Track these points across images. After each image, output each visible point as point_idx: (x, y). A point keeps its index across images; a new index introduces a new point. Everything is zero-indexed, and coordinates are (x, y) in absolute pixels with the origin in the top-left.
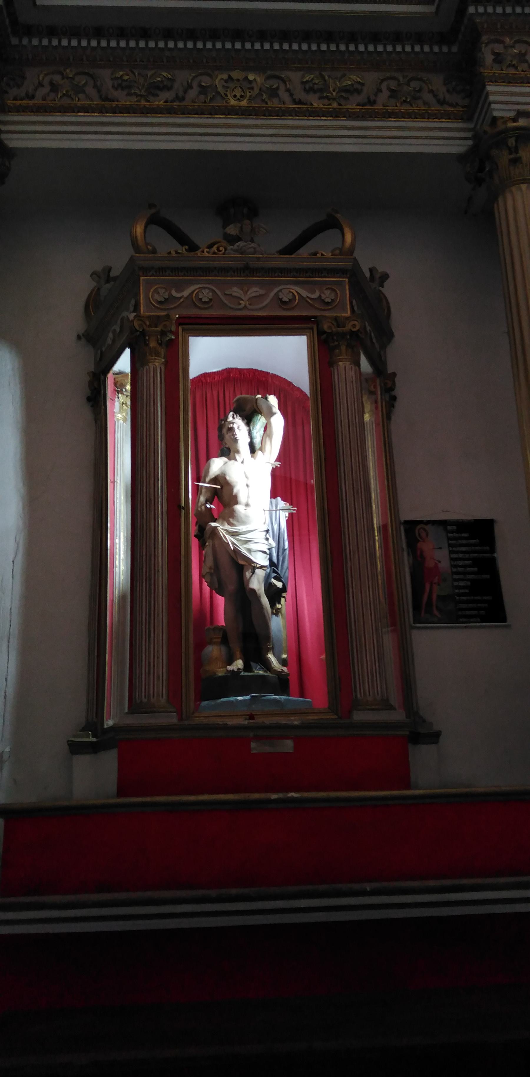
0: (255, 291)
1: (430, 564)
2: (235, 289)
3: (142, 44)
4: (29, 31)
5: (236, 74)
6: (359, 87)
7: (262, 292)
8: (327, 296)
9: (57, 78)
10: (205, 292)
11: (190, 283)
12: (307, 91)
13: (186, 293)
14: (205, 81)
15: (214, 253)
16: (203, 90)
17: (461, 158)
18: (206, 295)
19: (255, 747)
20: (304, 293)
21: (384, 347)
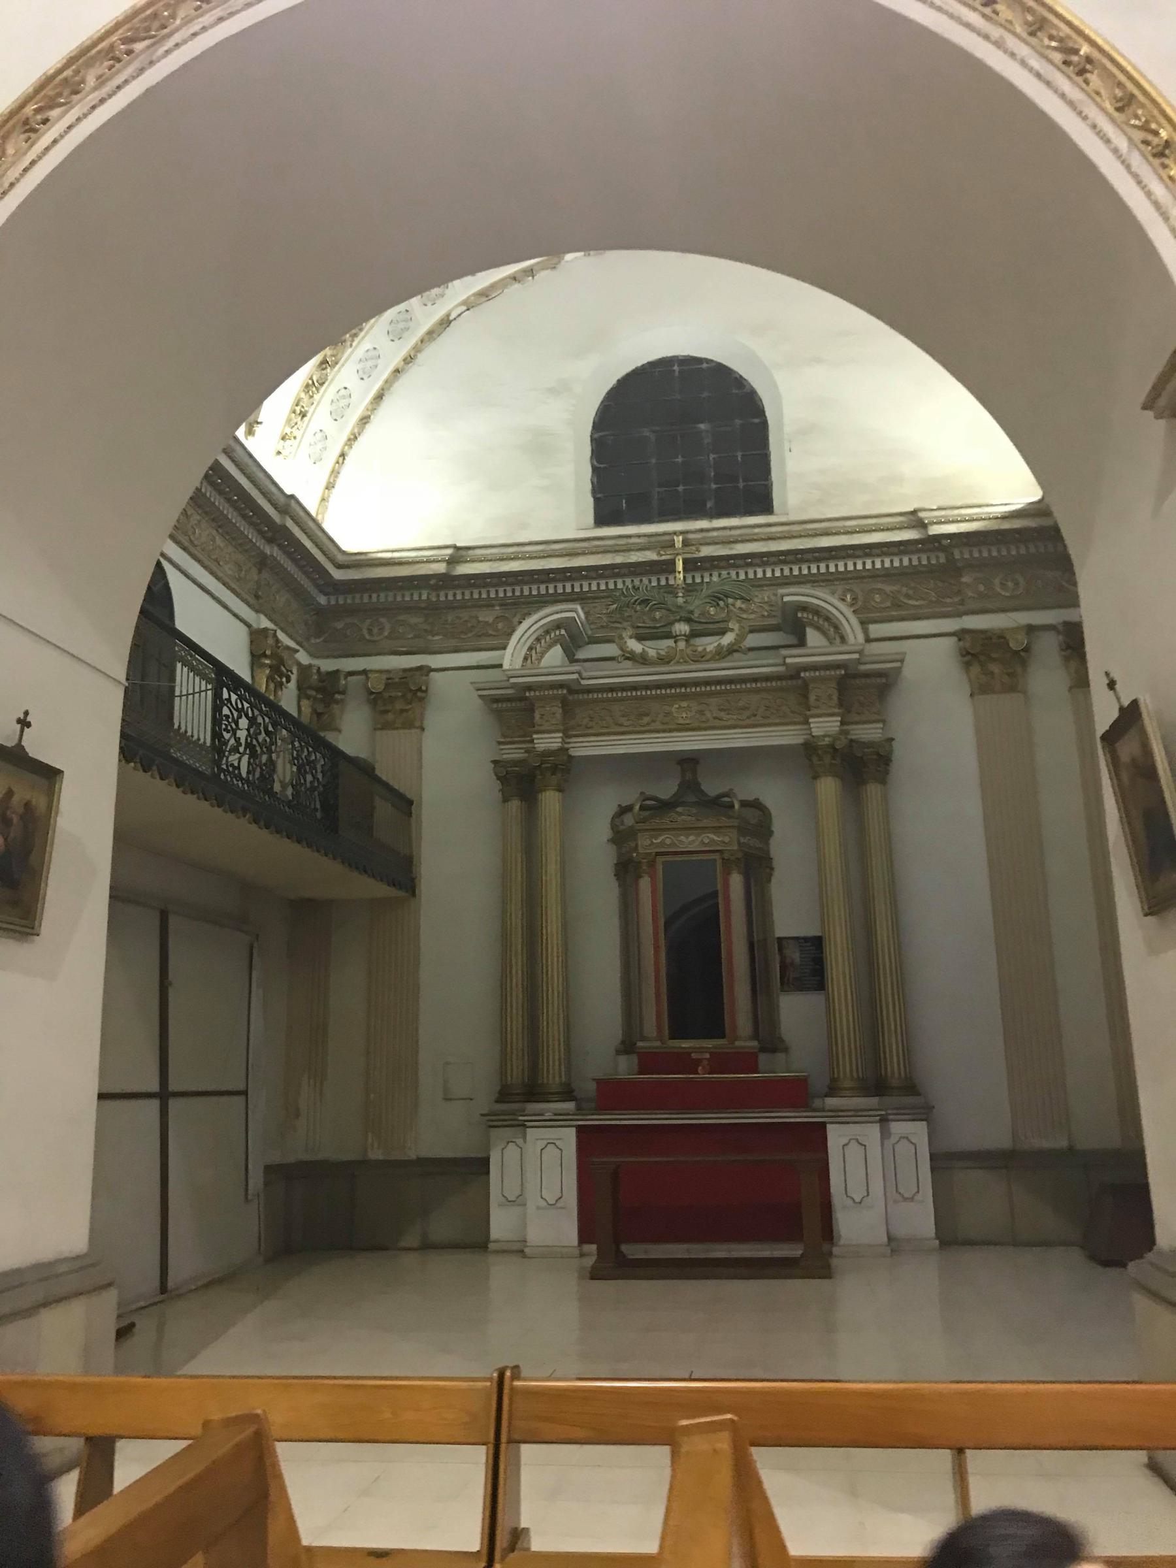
0: (692, 838)
1: (788, 961)
3: (634, 694)
5: (684, 704)
6: (747, 705)
8: (727, 839)
9: (591, 712)
10: (668, 839)
11: (660, 835)
12: (721, 710)
13: (659, 841)
14: (667, 708)
16: (667, 714)
17: (802, 744)
18: (668, 841)
19: (694, 1056)
20: (716, 838)
21: (767, 844)
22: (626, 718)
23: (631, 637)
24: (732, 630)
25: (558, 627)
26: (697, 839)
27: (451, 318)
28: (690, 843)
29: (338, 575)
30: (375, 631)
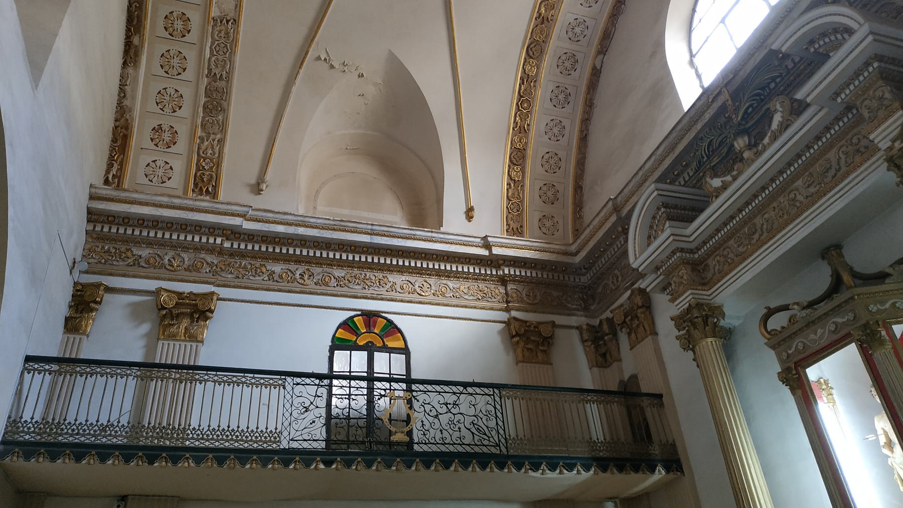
0: (820, 331)
2: (812, 335)
4: (698, 249)
6: (828, 166)
7: (822, 331)
13: (793, 349)
15: (793, 323)
20: (840, 320)
22: (742, 246)
23: (712, 179)
24: (776, 111)
25: (659, 209)
26: (825, 330)
27: (598, 68)
28: (821, 338)
29: (578, 259)
30: (615, 281)
